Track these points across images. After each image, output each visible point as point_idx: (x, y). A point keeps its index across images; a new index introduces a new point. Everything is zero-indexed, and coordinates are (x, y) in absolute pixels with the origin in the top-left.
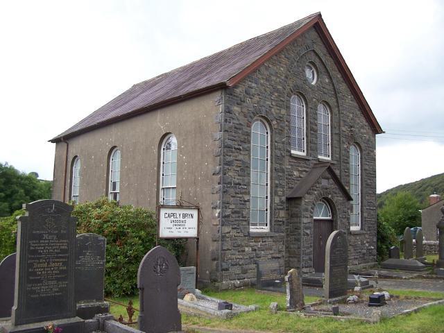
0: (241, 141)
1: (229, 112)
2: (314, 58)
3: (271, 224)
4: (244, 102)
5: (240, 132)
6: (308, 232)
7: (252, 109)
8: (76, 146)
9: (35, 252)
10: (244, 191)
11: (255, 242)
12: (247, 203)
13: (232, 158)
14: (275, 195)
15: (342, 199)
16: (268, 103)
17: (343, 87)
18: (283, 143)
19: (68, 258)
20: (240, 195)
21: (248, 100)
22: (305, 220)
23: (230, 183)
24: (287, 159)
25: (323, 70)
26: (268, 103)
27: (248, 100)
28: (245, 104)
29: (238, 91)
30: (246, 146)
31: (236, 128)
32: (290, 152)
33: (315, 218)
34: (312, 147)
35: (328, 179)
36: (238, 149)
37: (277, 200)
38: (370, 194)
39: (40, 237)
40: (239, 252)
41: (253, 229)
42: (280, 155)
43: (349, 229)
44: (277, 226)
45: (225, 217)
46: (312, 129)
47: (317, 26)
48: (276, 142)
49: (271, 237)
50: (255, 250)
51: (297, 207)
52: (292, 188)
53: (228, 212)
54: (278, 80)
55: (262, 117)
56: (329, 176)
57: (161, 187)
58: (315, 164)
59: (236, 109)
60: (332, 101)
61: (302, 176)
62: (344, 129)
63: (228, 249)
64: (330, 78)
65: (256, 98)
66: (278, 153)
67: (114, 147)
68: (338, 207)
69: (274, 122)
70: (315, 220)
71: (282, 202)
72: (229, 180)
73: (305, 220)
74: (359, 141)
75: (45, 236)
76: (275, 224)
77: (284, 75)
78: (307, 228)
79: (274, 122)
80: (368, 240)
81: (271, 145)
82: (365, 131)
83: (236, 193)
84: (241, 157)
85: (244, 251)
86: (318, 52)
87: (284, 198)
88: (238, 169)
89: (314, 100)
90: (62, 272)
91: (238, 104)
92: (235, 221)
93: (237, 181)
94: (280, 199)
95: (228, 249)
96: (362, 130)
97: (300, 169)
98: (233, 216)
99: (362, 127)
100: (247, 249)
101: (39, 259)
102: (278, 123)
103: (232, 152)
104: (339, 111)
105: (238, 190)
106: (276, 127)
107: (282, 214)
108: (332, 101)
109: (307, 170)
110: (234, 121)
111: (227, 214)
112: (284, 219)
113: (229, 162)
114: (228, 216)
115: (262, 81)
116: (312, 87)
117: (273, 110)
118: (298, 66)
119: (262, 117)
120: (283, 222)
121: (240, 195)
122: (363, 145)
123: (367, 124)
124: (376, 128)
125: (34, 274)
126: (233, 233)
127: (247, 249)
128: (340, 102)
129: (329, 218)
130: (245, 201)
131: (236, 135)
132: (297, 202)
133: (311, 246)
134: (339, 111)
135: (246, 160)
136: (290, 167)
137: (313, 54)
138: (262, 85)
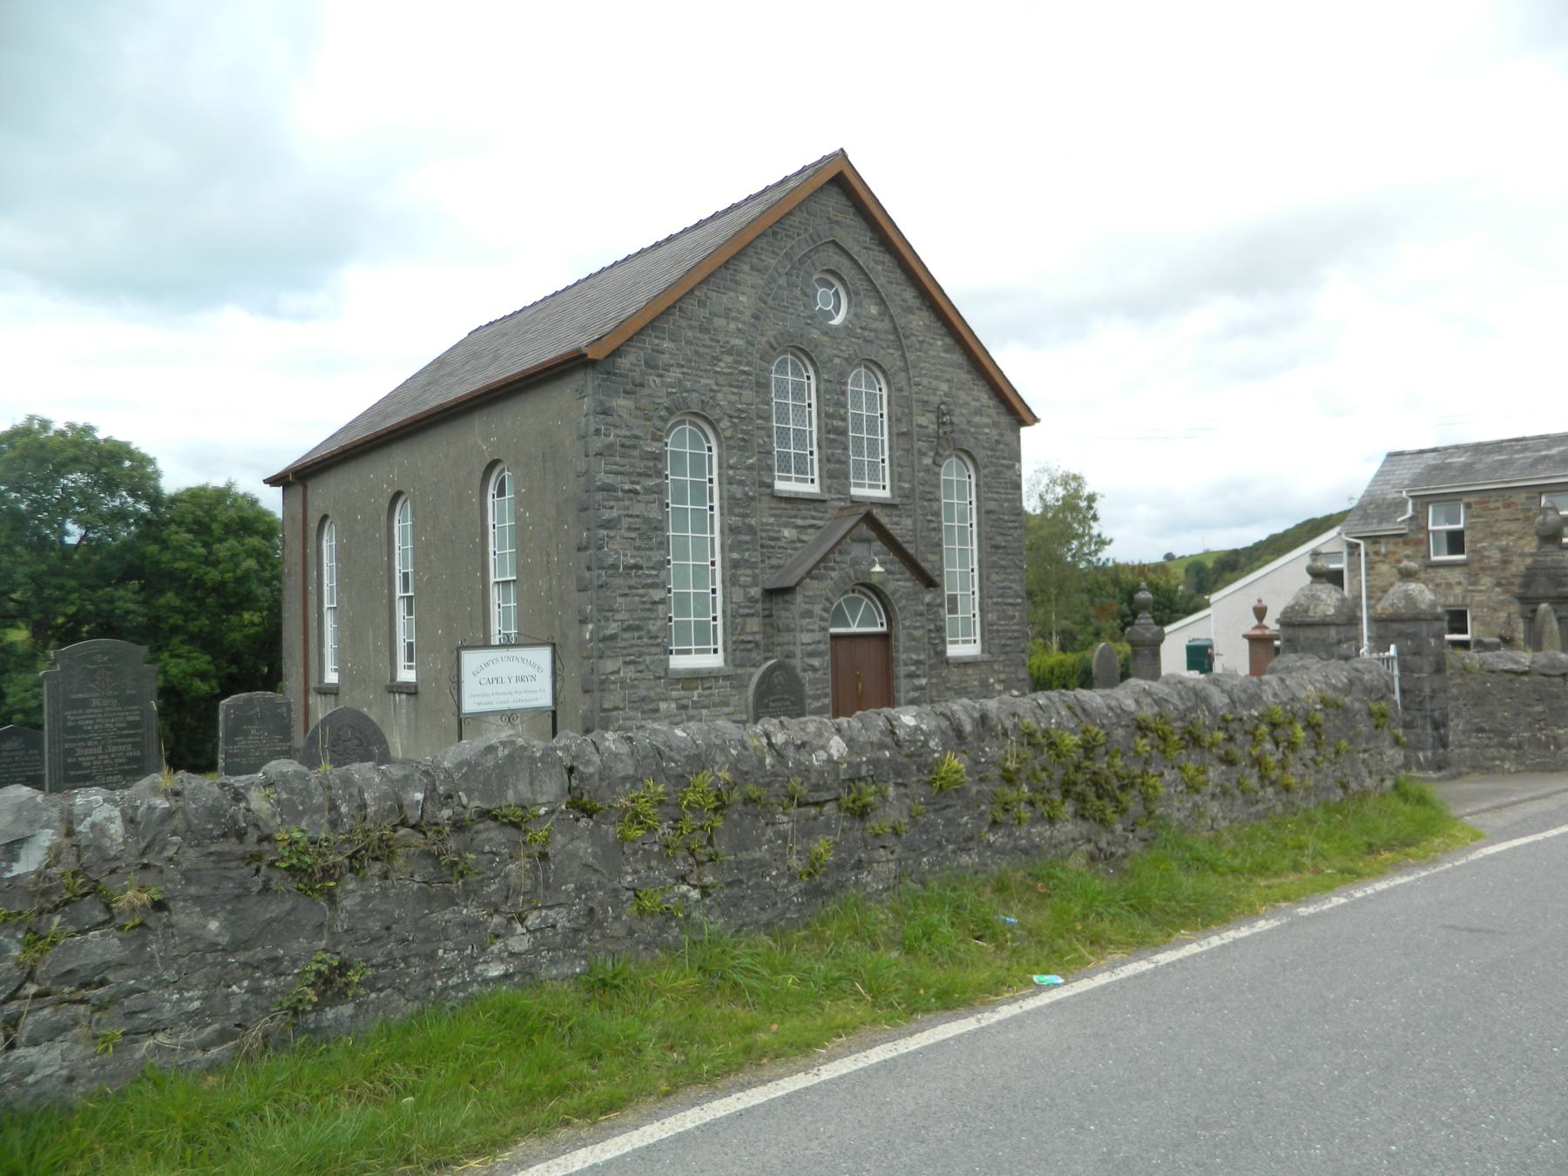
0: (640, 474)
1: (604, 413)
2: (835, 260)
3: (725, 650)
4: (642, 385)
5: (636, 453)
6: (816, 662)
7: (666, 402)
8: (323, 494)
9: (75, 730)
10: (649, 581)
11: (683, 689)
12: (661, 607)
13: (615, 513)
14: (733, 585)
15: (909, 584)
16: (704, 381)
17: (919, 321)
18: (750, 468)
19: (142, 735)
20: (641, 591)
21: (653, 380)
22: (806, 638)
23: (614, 566)
24: (765, 503)
25: (862, 286)
26: (704, 381)
27: (653, 380)
28: (646, 391)
29: (625, 362)
30: (651, 483)
31: (623, 446)
32: (771, 486)
33: (833, 630)
34: (835, 472)
35: (868, 541)
36: (630, 491)
37: (738, 596)
38: (1004, 567)
39: (84, 704)
40: (643, 712)
41: (678, 662)
42: (749, 497)
43: (944, 652)
44: (738, 654)
45: (605, 639)
46: (834, 434)
47: (838, 184)
48: (730, 467)
49: (726, 678)
50: (685, 707)
51: (786, 610)
52: (779, 567)
53: (613, 628)
54: (732, 326)
55: (696, 414)
56: (872, 535)
57: (492, 580)
58: (842, 509)
59: (622, 403)
60: (890, 358)
61: (804, 537)
62: (923, 421)
63: (616, 708)
64: (882, 302)
65: (674, 375)
66: (738, 491)
67: (397, 495)
68: (899, 604)
69: (725, 424)
70: (835, 637)
71: (752, 600)
72: (610, 561)
73: (806, 638)
74: (968, 444)
75: (95, 702)
76: (738, 649)
77: (748, 313)
78: (811, 655)
79: (725, 424)
80: (1002, 676)
81: (720, 475)
82: (986, 420)
83: (630, 587)
84: (638, 509)
85: (657, 710)
86: (849, 244)
87: (755, 592)
88: (633, 535)
89: (837, 361)
90: (131, 760)
91: (626, 392)
92: (632, 646)
93: (632, 561)
94: (746, 594)
95: (616, 708)
96: (977, 419)
97: (800, 522)
98: (627, 635)
99: (978, 412)
100: (663, 706)
101: (85, 740)
102: (734, 426)
103: (617, 499)
104: (909, 379)
105: (632, 582)
106: (728, 433)
107: (754, 625)
108: (890, 358)
109: (819, 523)
110: (618, 431)
111: (609, 632)
112: (758, 637)
113: (609, 521)
114: (613, 637)
115: (690, 334)
116: (831, 332)
117: (719, 396)
118: (791, 285)
119: (696, 414)
120: (757, 644)
121: (641, 591)
122: (981, 455)
123: (992, 403)
124: (1017, 414)
125: (77, 766)
126: (629, 673)
127: (663, 706)
128: (911, 356)
129: (879, 629)
130: (654, 603)
131: (623, 461)
132: (788, 597)
133: (826, 695)
134: (909, 379)
135: (654, 514)
136: (772, 520)
137: (832, 249)
138: (689, 342)
